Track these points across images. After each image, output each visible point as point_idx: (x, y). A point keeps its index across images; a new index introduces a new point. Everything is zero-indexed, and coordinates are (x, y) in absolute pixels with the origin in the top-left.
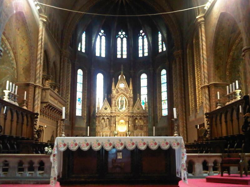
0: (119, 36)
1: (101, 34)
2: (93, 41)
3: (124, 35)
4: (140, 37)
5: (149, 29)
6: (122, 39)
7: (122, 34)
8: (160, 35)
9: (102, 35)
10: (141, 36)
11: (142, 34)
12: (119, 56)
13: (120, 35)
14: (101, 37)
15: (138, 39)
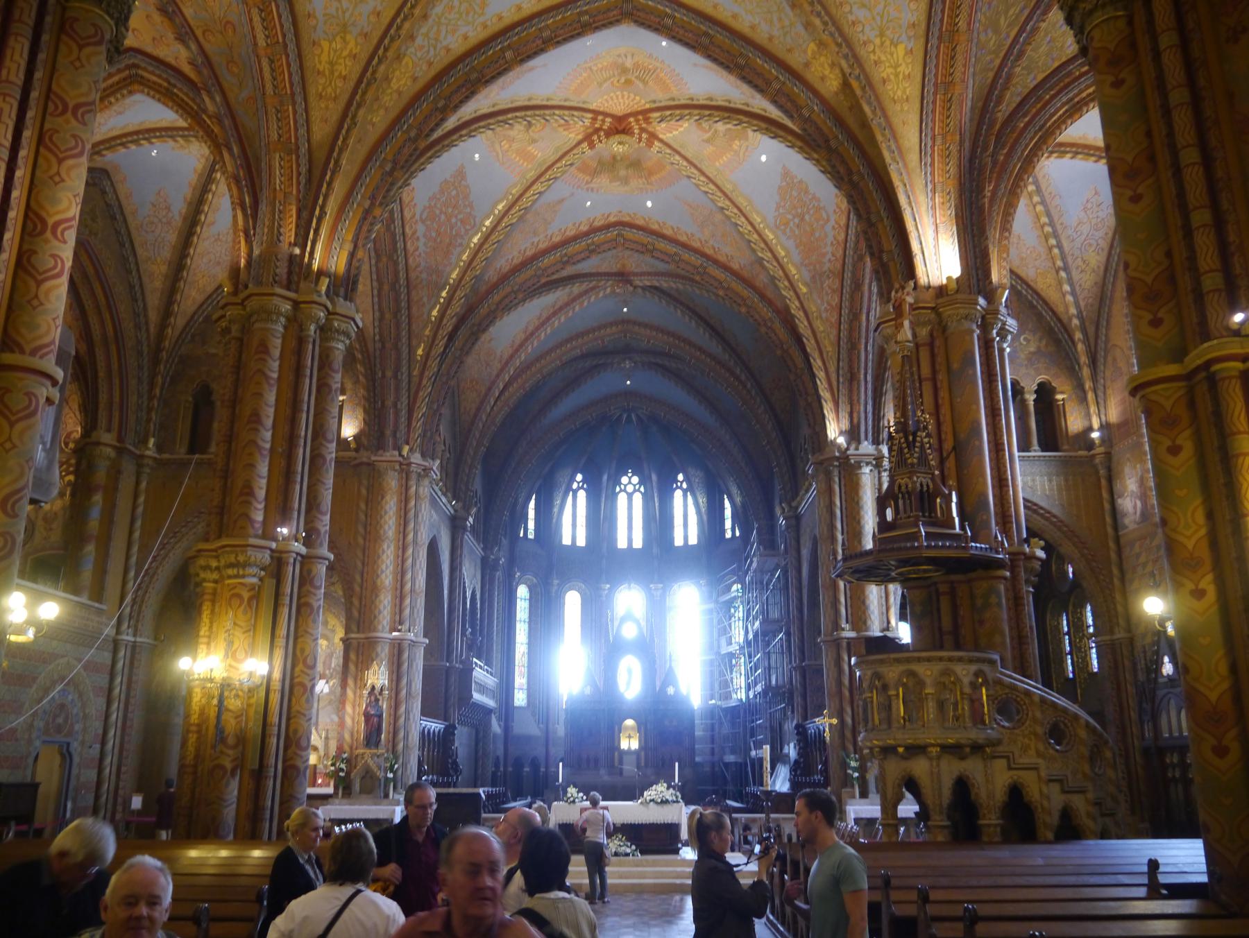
0: (623, 487)
1: (575, 486)
2: (556, 510)
3: (635, 485)
4: (678, 494)
5: (698, 476)
6: (630, 496)
7: (630, 481)
8: (727, 504)
9: (579, 488)
10: (681, 488)
11: (682, 483)
12: (622, 543)
13: (625, 486)
14: (575, 492)
15: (672, 497)
